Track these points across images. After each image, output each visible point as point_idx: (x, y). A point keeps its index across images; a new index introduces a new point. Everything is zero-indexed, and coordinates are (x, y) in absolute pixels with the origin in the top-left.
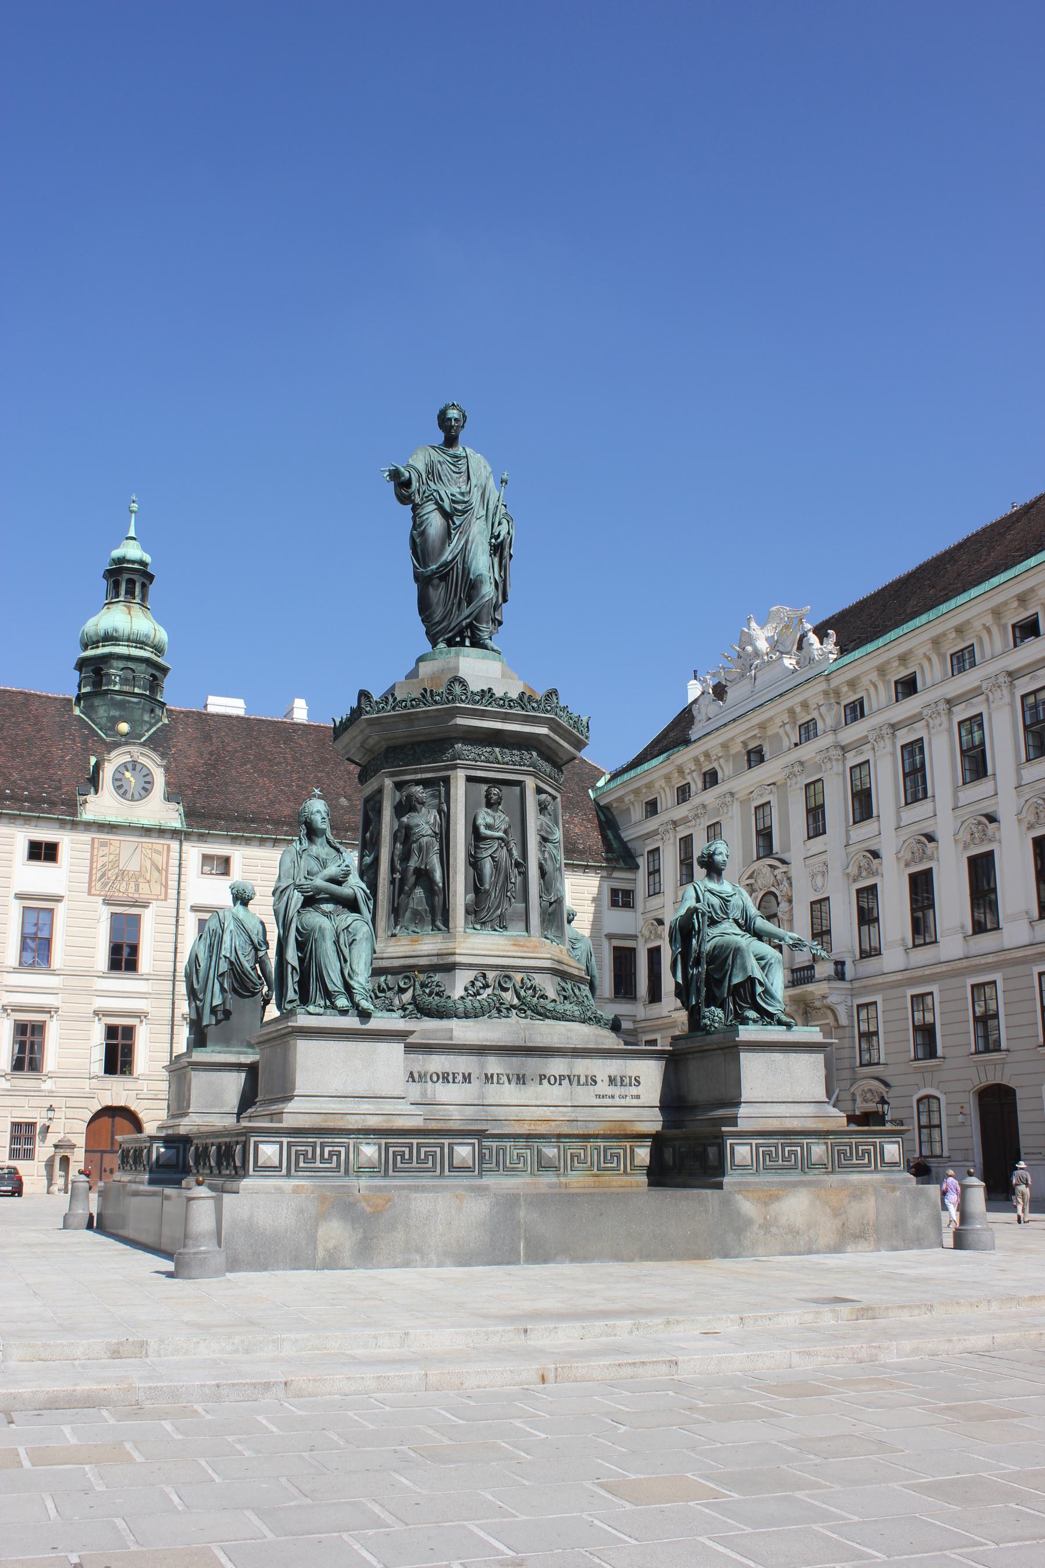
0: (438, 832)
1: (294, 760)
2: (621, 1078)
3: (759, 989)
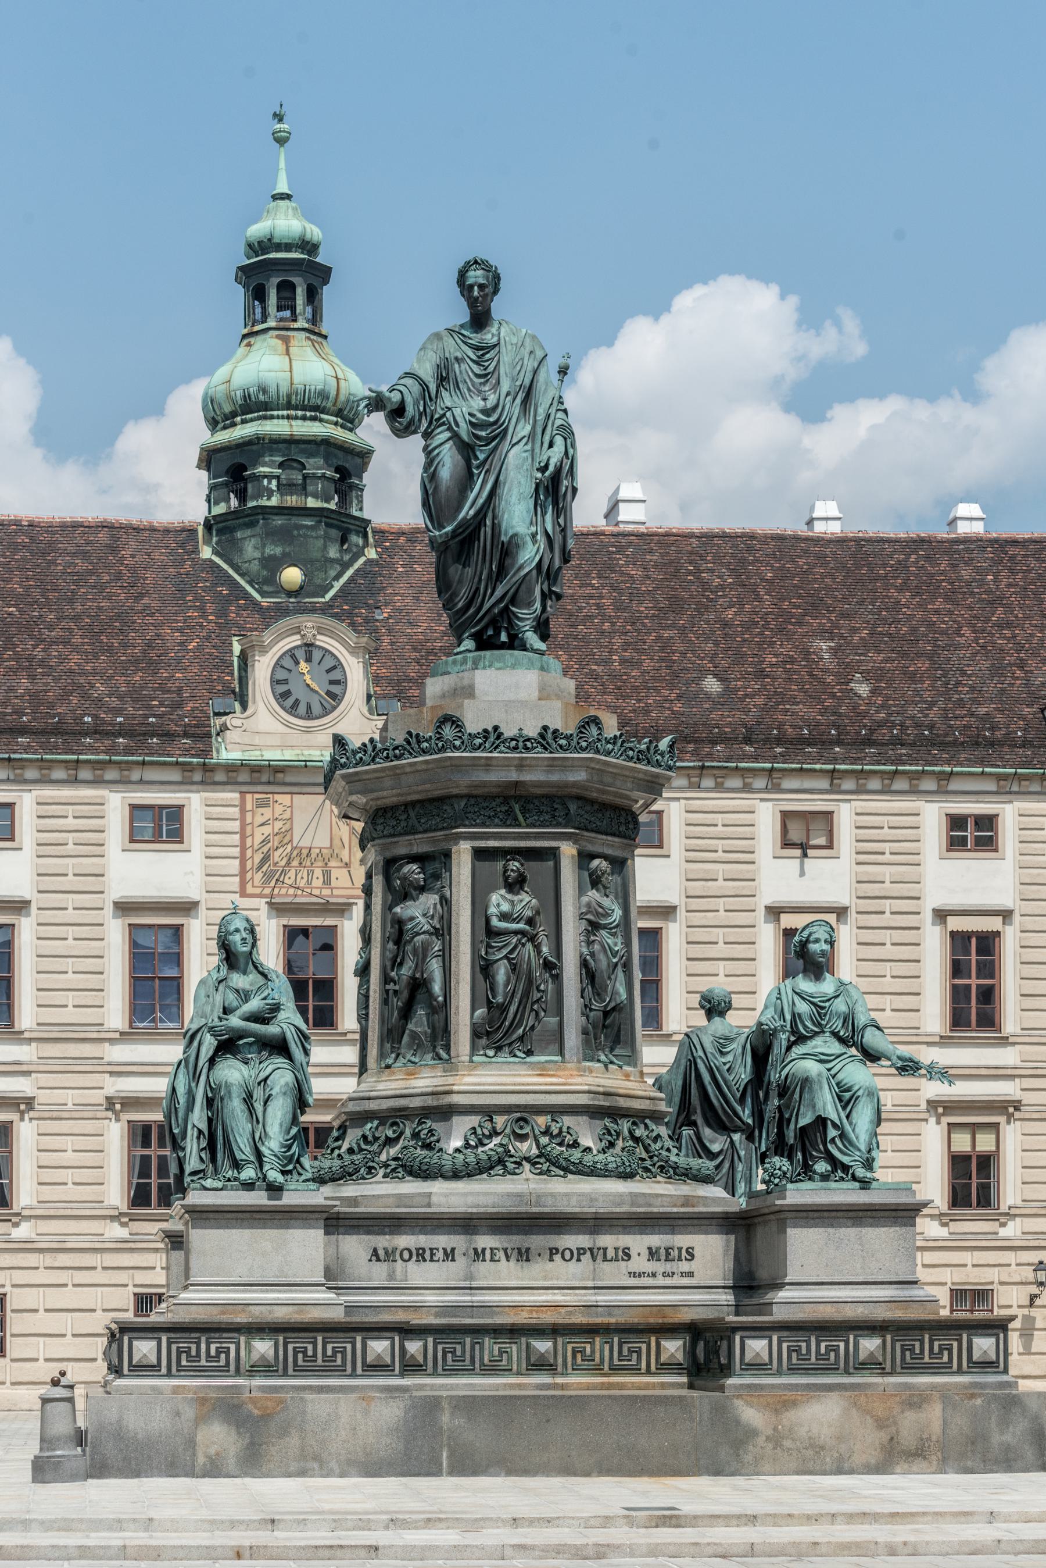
0: (438, 926)
1: (617, 609)
2: (667, 1250)
3: (832, 1133)
